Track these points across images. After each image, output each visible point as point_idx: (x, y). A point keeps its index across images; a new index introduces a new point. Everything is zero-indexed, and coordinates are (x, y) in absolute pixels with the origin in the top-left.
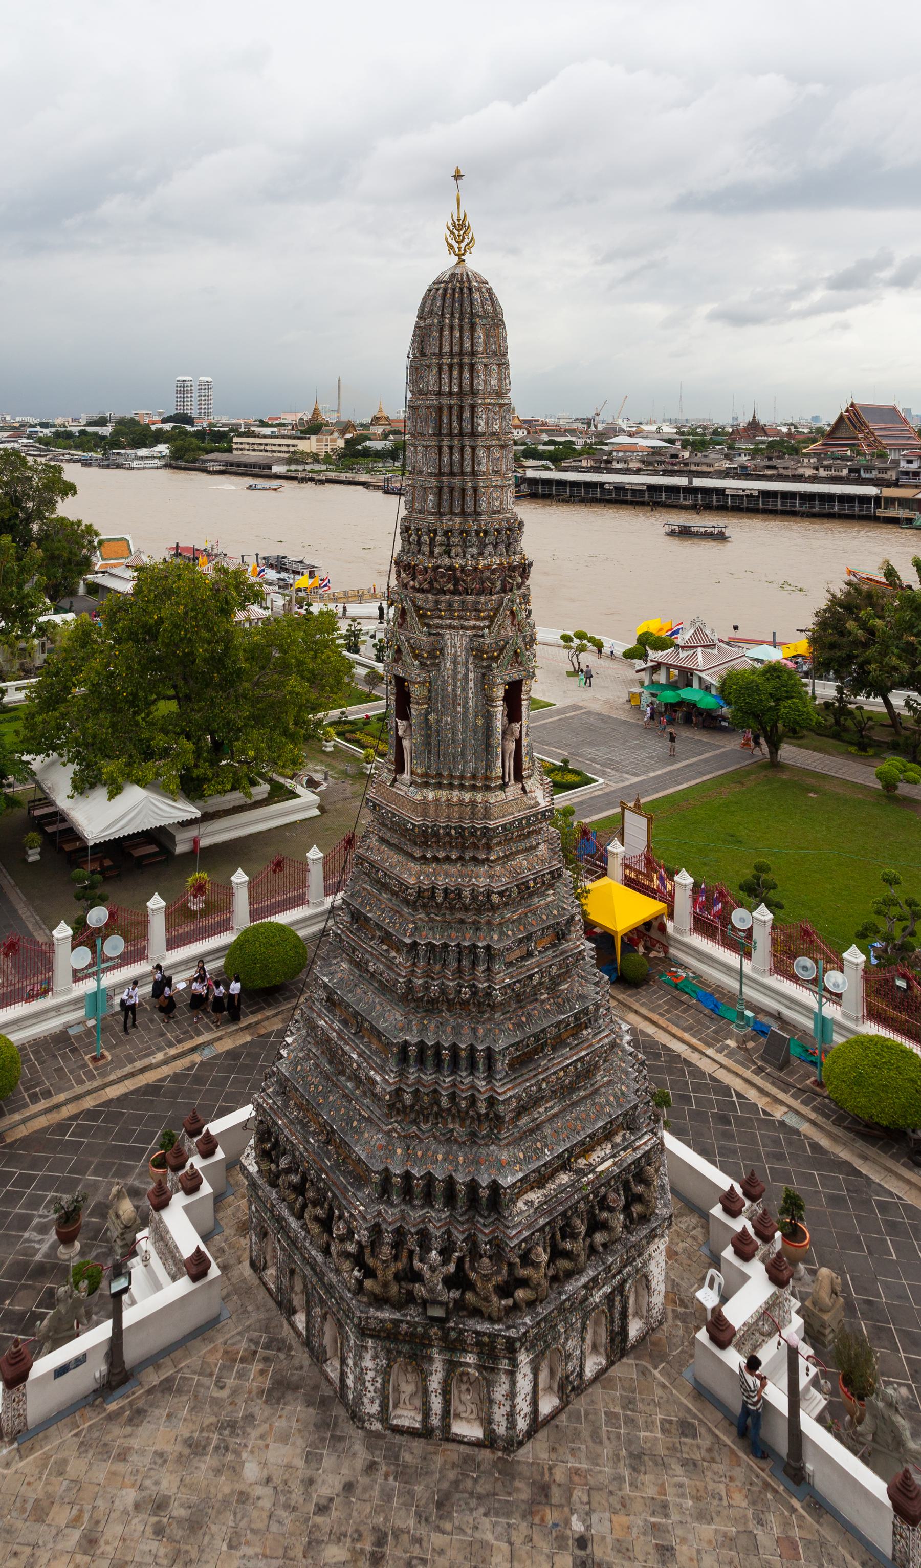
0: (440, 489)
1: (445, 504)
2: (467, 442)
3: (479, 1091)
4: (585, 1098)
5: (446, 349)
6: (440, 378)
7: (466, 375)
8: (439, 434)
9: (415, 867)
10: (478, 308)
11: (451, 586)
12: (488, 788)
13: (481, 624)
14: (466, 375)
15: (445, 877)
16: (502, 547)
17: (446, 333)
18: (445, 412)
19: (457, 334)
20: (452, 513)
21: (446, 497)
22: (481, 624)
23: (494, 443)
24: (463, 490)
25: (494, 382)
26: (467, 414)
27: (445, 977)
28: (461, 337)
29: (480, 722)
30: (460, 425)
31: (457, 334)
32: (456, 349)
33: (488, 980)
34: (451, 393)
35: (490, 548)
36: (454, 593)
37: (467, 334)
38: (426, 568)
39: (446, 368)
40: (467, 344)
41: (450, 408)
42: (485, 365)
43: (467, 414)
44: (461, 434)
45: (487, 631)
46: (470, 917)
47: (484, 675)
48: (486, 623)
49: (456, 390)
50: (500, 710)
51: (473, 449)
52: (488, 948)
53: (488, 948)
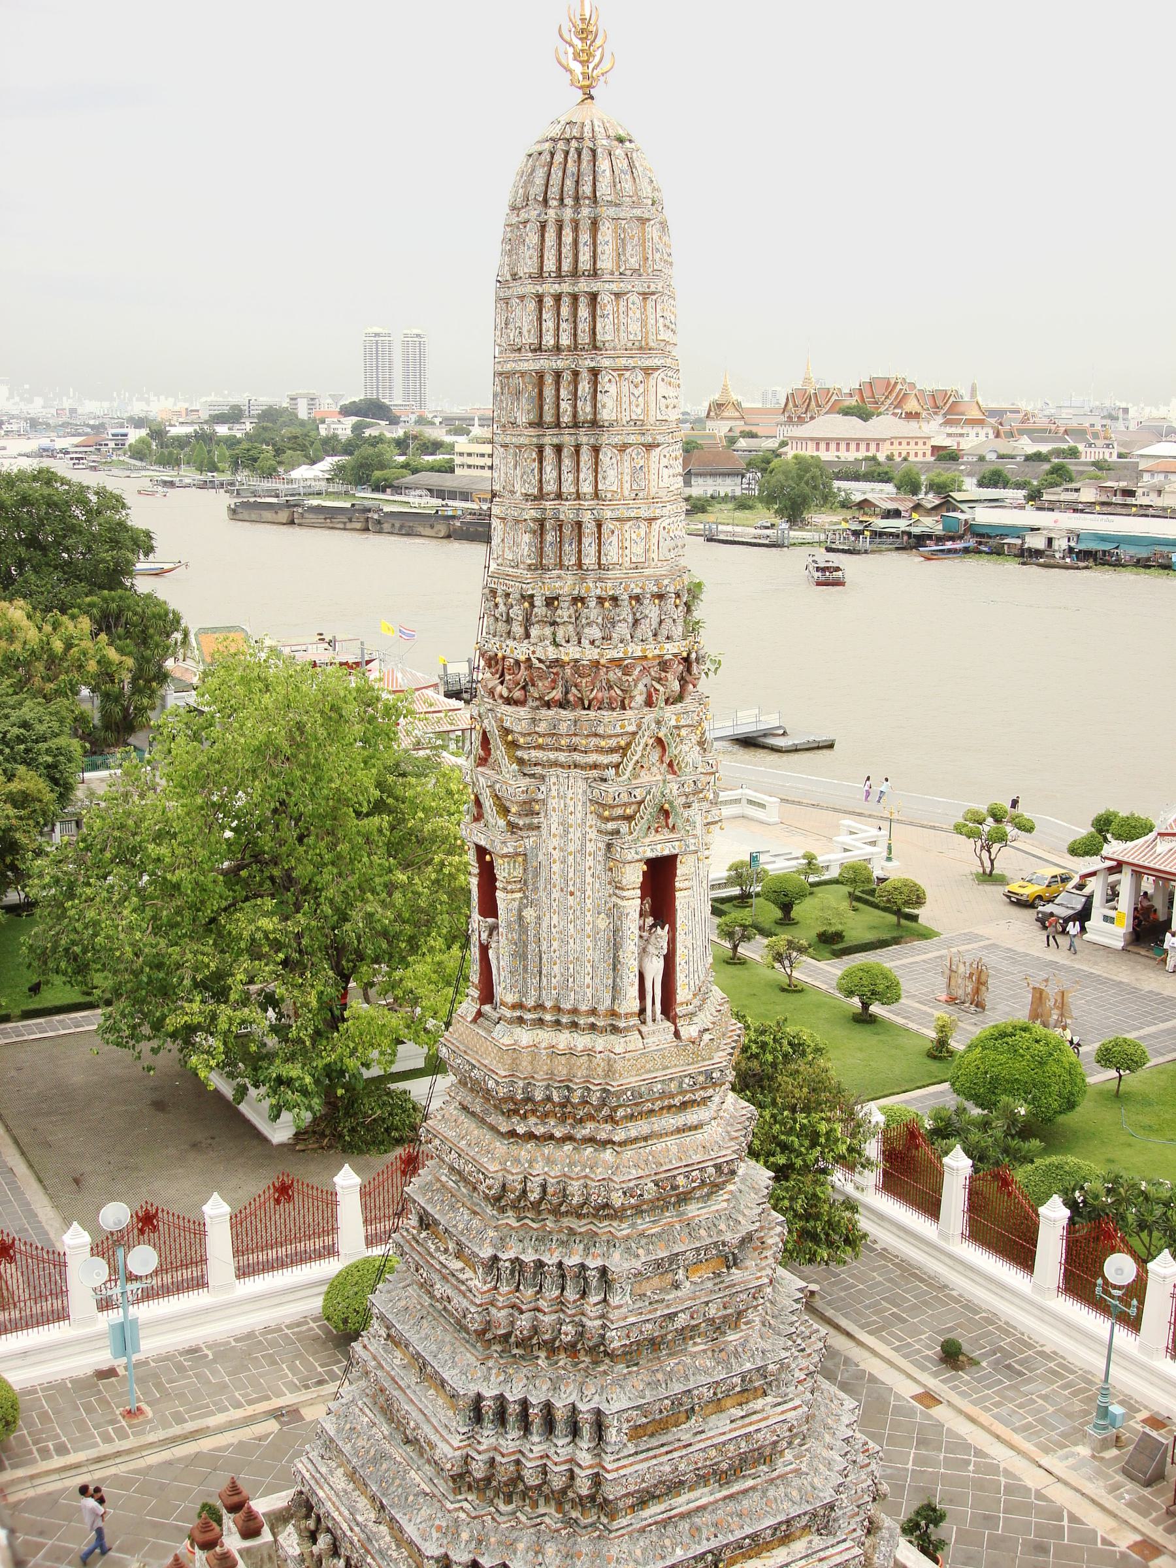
0: (541, 523)
3: (580, 1466)
4: (753, 1488)
5: (550, 265)
6: (540, 319)
7: (584, 312)
8: (539, 423)
9: (501, 1147)
10: (604, 189)
11: (557, 694)
12: (615, 1030)
13: (604, 759)
14: (584, 312)
15: (545, 1166)
16: (645, 629)
17: (551, 235)
18: (549, 379)
19: (568, 237)
20: (561, 566)
21: (549, 537)
22: (604, 759)
23: (632, 439)
24: (579, 524)
25: (635, 327)
26: (584, 387)
27: (538, 1310)
28: (576, 242)
31: (568, 237)
32: (566, 266)
33: (602, 1316)
34: (558, 348)
35: (623, 629)
36: (563, 704)
37: (585, 237)
38: (517, 663)
39: (549, 302)
42: (618, 295)
43: (584, 387)
44: (576, 425)
45: (612, 771)
46: (580, 1226)
47: (609, 846)
48: (615, 758)
49: (565, 341)
50: (632, 904)
51: (596, 450)
52: (603, 1271)
53: (603, 1271)
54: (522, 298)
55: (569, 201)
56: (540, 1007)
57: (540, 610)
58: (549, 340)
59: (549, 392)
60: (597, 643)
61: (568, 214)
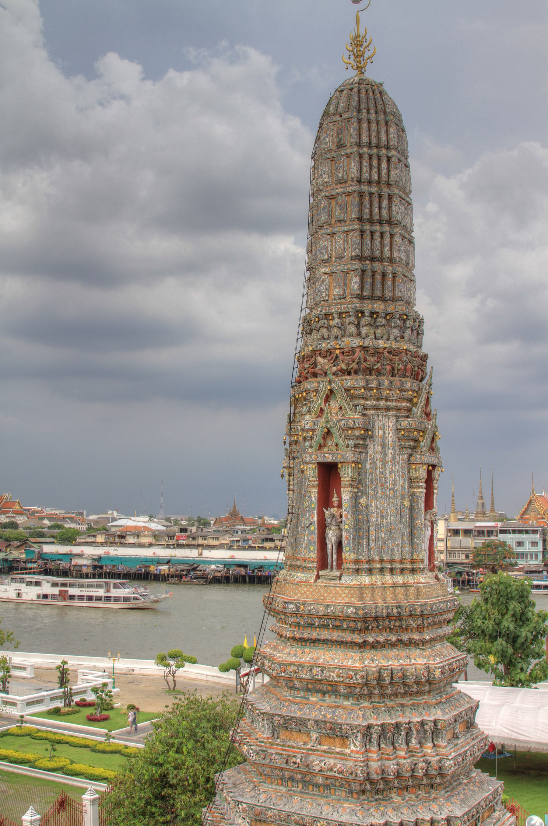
0: (363, 271)
1: (368, 286)
2: (386, 228)
7: (384, 165)
8: (360, 219)
14: (384, 165)
19: (374, 126)
26: (385, 203)
29: (407, 503)
30: (380, 211)
40: (384, 138)
41: (371, 195)
43: (385, 203)
49: (375, 177)
51: (392, 236)
54: (348, 156)
55: (372, 111)
56: (369, 561)
57: (367, 319)
58: (366, 176)
59: (366, 202)
60: (398, 339)
61: (373, 116)
